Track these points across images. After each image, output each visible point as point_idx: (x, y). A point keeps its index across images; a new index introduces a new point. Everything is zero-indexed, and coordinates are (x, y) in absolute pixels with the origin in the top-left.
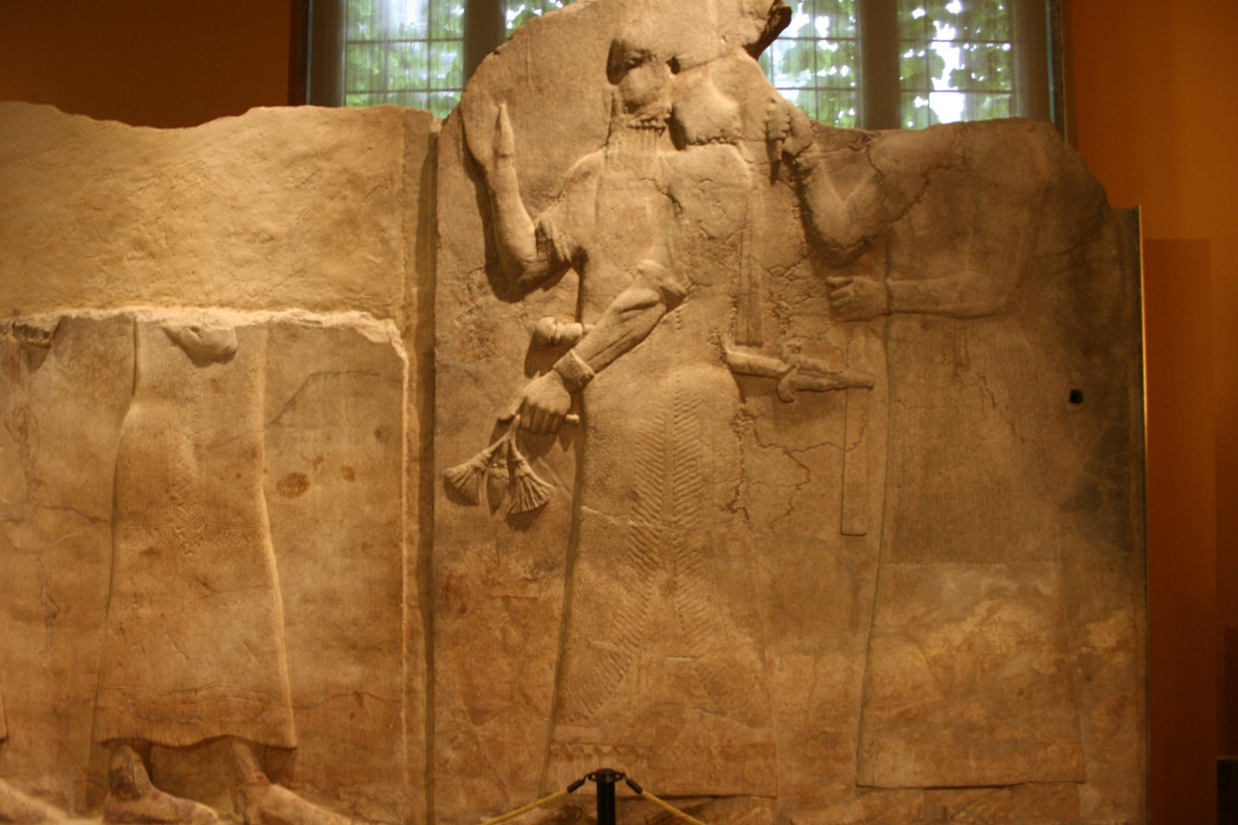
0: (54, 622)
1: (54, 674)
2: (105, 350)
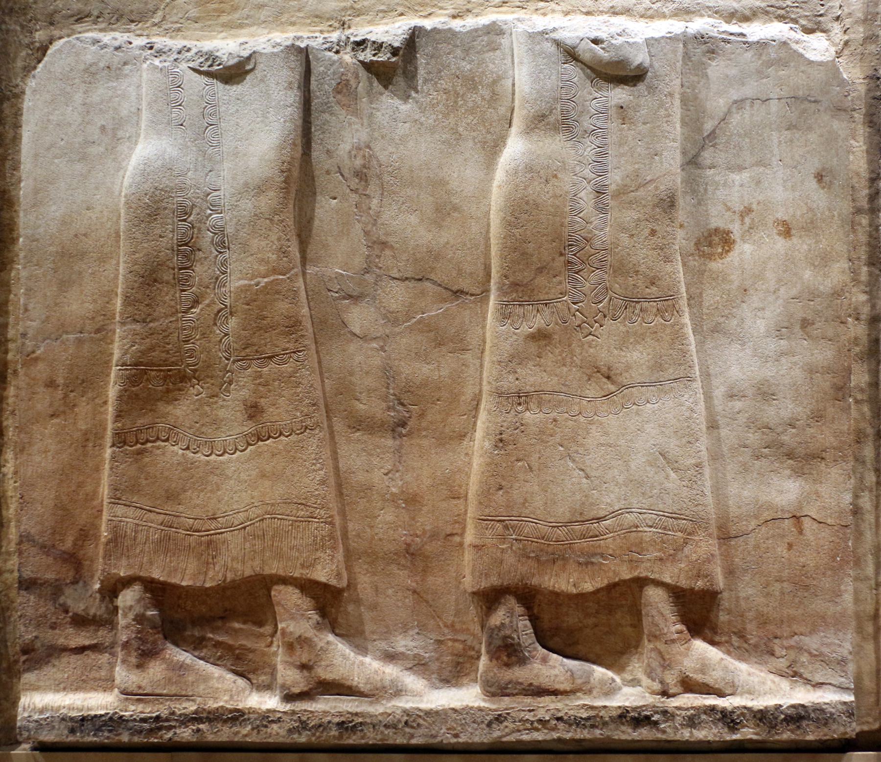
0: (404, 431)
1: (406, 501)
2: (471, 70)
